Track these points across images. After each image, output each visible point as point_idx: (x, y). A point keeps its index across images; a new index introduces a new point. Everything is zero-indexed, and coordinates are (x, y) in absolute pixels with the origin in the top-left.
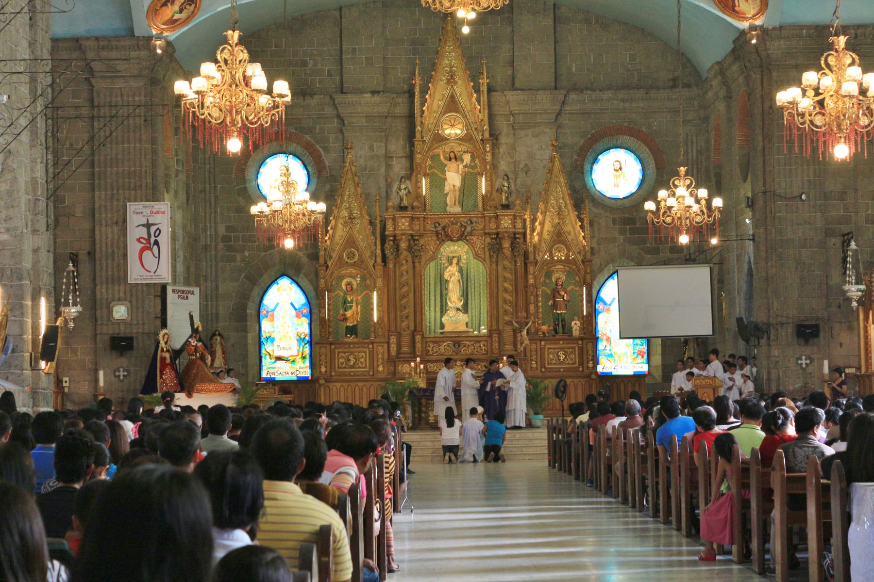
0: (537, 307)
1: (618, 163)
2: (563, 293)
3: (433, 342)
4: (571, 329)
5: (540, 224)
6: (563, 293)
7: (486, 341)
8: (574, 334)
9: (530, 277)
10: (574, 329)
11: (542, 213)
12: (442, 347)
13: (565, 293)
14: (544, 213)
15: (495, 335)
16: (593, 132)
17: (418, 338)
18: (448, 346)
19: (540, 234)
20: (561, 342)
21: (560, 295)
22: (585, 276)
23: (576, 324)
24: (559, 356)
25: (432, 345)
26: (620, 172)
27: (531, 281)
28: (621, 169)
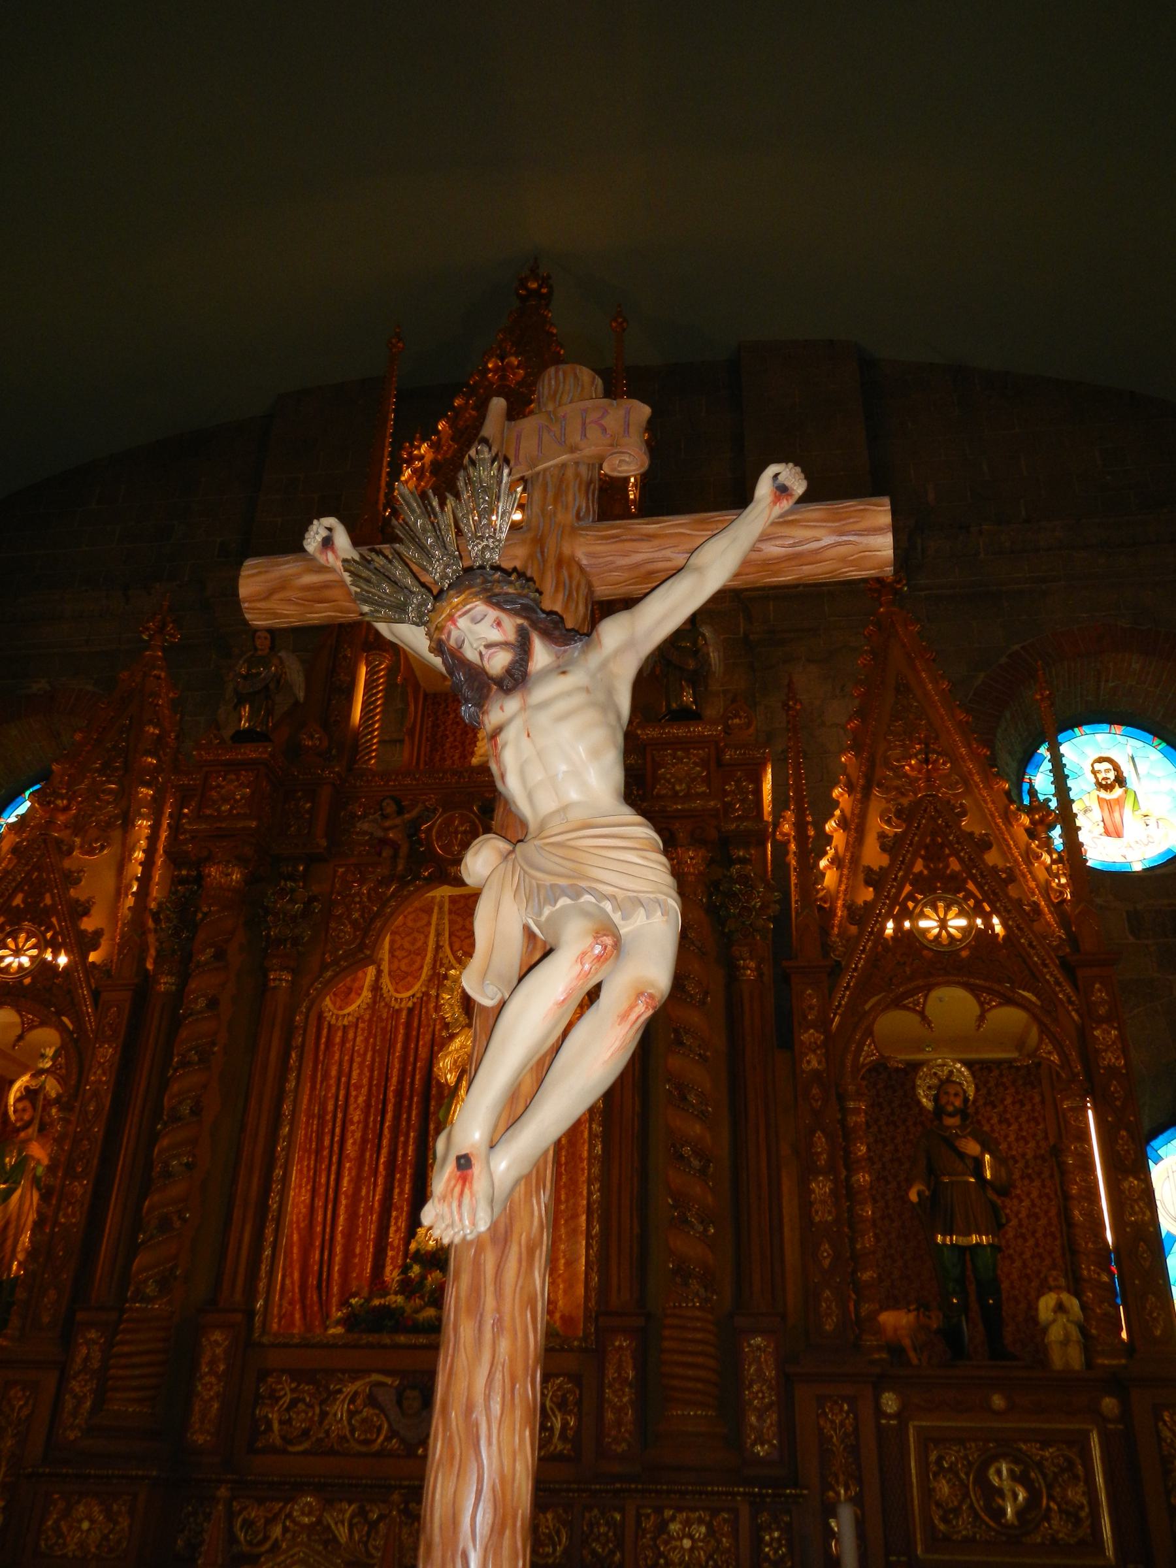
0: (846, 1192)
1: (1106, 765)
2: (972, 1147)
3: (298, 1375)
4: (1035, 1330)
5: (843, 824)
6: (972, 1147)
7: (576, 1379)
8: (1057, 1360)
9: (809, 1036)
10: (1055, 1334)
11: (850, 788)
12: (340, 1409)
13: (986, 1148)
14: (863, 791)
15: (621, 1342)
16: (1016, 647)
17: (217, 1342)
18: (372, 1401)
19: (848, 863)
20: (998, 1401)
21: (962, 1155)
22: (1083, 1036)
23: (1060, 1308)
24: (992, 1494)
25: (286, 1390)
26: (1118, 792)
27: (813, 1062)
28: (1120, 780)
